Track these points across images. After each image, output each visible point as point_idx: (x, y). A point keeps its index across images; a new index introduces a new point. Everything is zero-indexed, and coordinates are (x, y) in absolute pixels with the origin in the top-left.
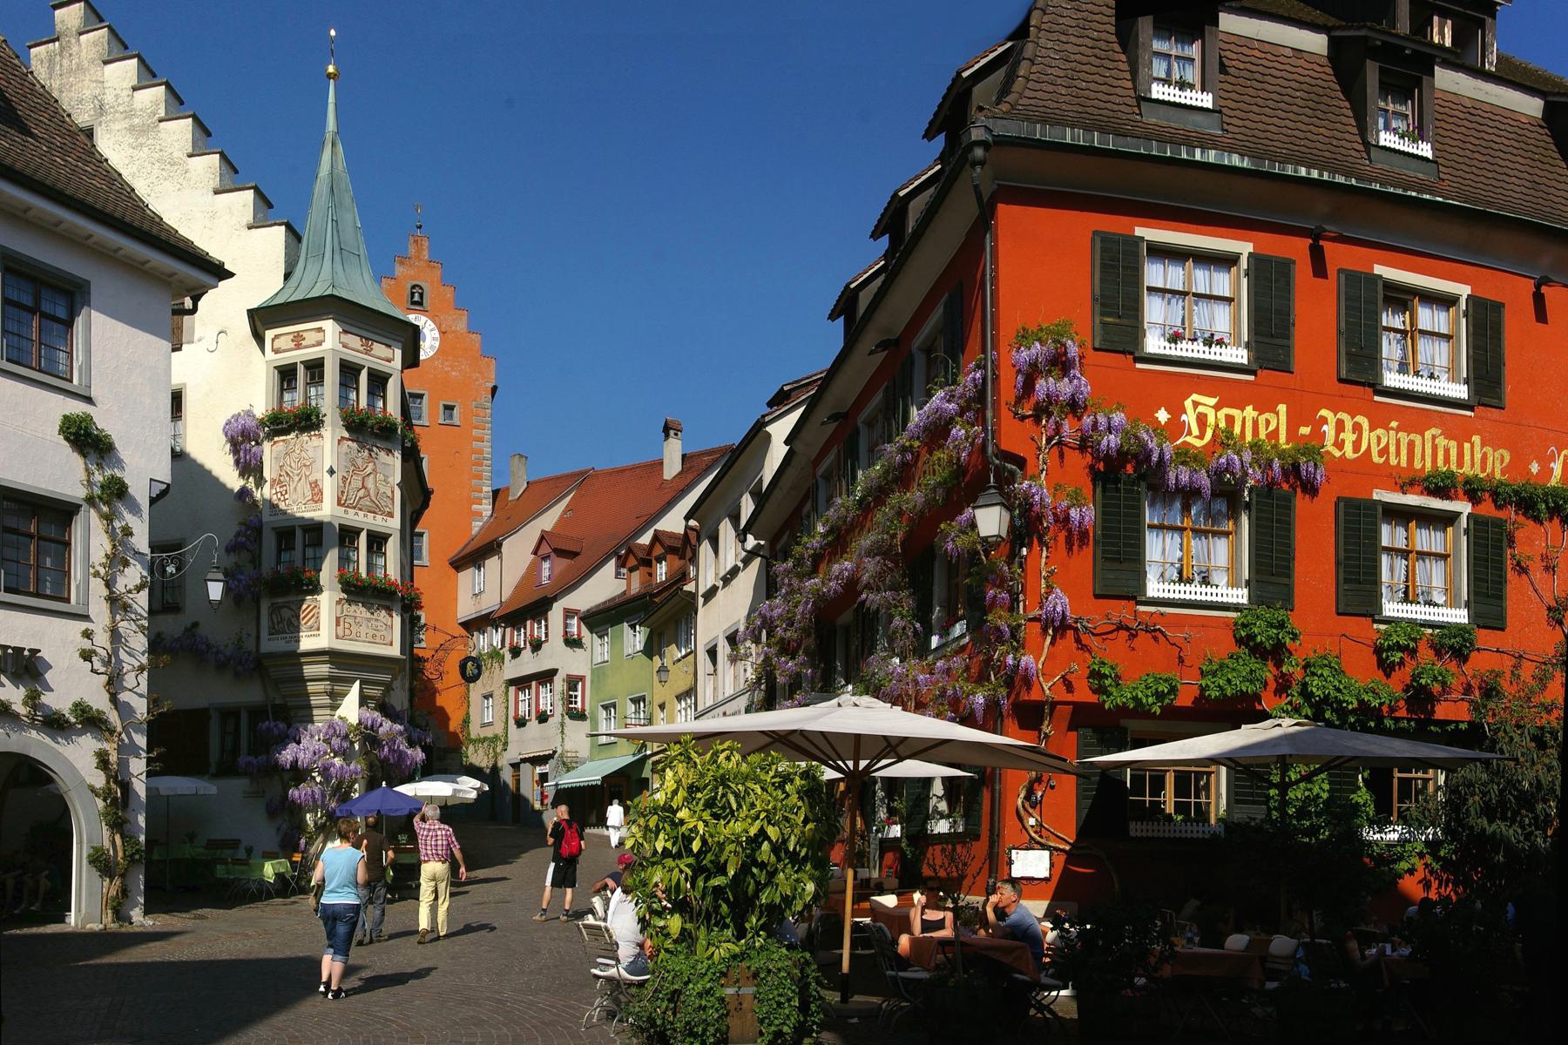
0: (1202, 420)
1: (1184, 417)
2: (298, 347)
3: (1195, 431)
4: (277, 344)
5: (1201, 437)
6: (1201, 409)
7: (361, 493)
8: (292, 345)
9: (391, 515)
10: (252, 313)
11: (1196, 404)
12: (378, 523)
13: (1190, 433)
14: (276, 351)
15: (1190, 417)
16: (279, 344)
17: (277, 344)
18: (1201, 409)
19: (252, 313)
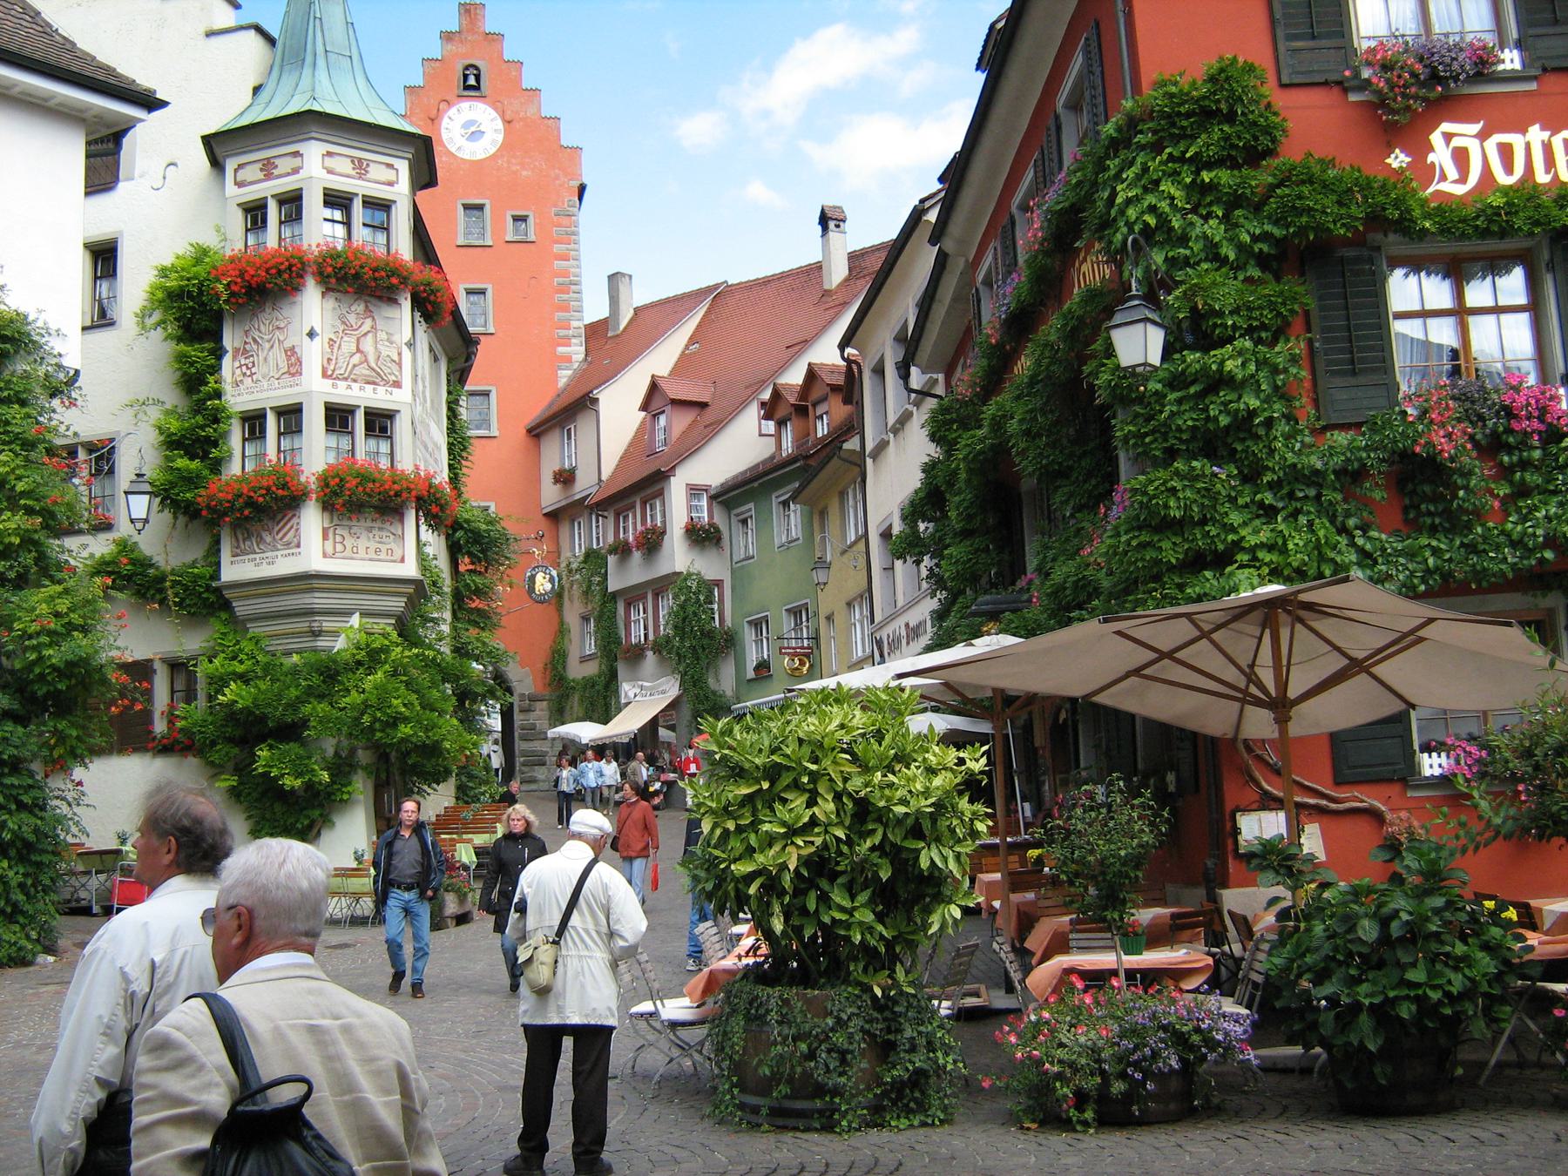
0: (1461, 157)
1: (1431, 158)
2: (269, 176)
3: (1452, 173)
4: (241, 176)
5: (1463, 179)
6: (1456, 142)
7: (357, 359)
8: (261, 175)
9: (397, 384)
10: (208, 141)
11: (1448, 137)
12: (379, 398)
13: (1443, 178)
14: (240, 184)
15: (1440, 155)
16: (243, 175)
17: (241, 176)
18: (1456, 142)
19: (208, 141)
